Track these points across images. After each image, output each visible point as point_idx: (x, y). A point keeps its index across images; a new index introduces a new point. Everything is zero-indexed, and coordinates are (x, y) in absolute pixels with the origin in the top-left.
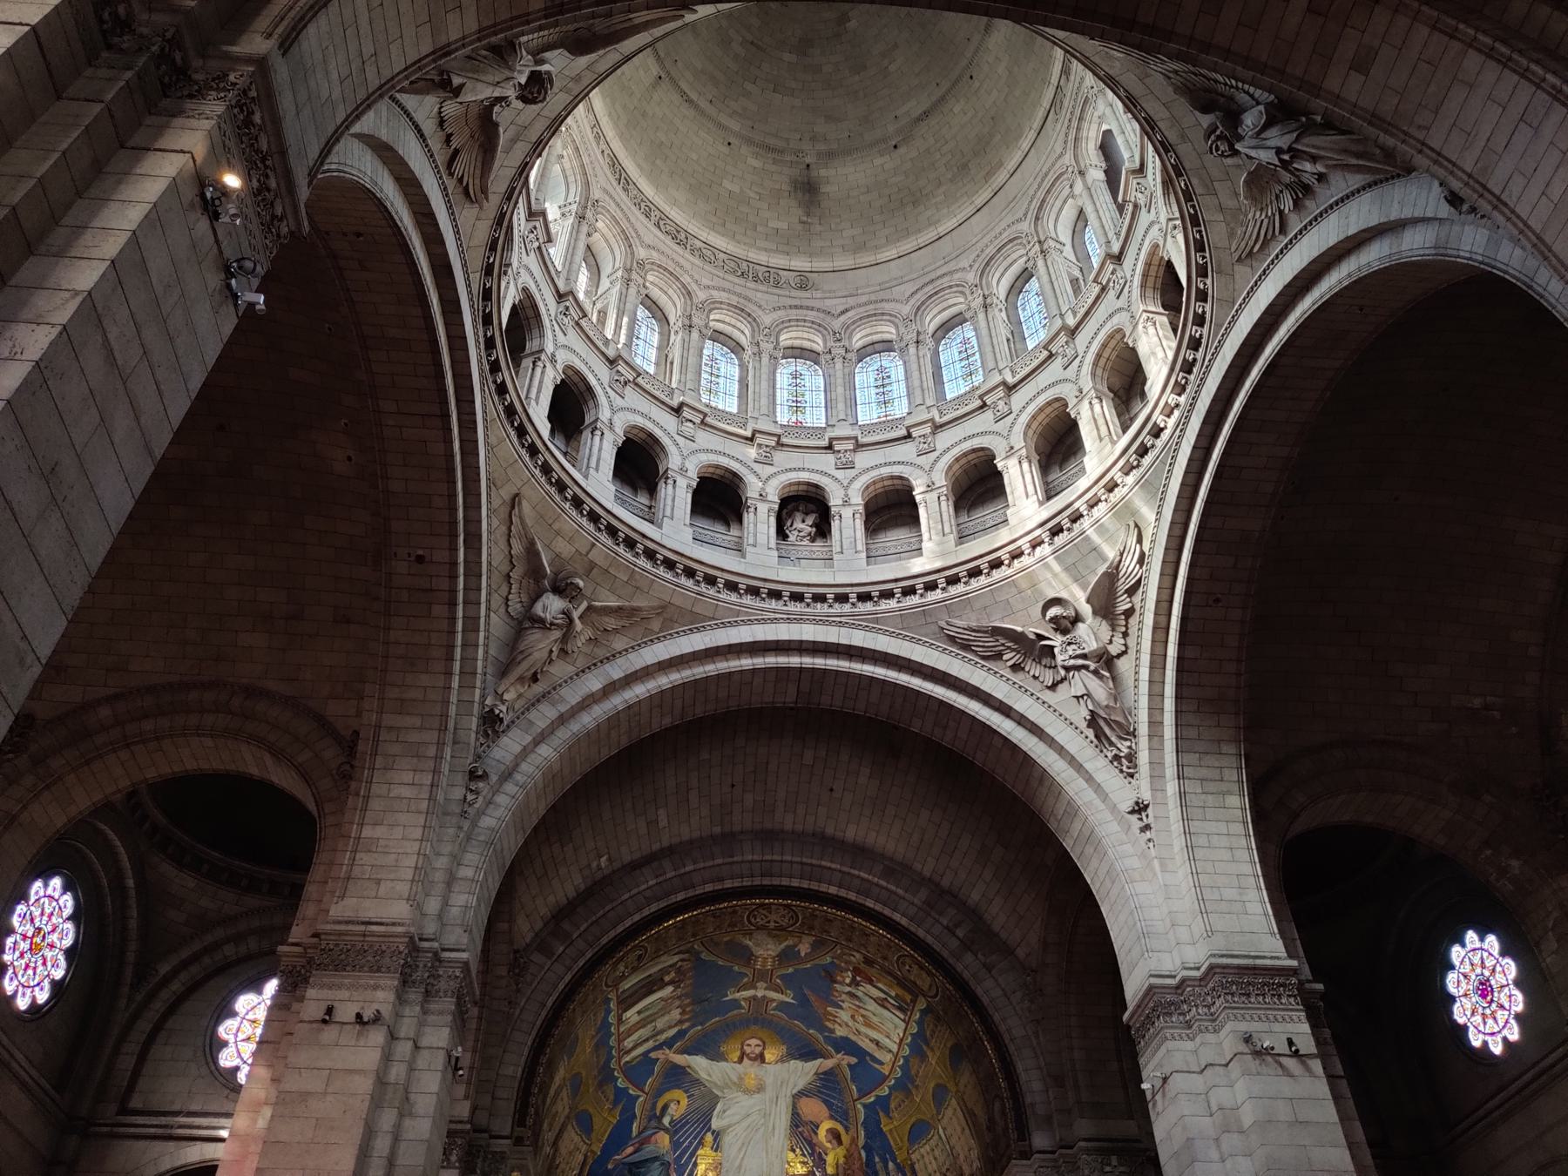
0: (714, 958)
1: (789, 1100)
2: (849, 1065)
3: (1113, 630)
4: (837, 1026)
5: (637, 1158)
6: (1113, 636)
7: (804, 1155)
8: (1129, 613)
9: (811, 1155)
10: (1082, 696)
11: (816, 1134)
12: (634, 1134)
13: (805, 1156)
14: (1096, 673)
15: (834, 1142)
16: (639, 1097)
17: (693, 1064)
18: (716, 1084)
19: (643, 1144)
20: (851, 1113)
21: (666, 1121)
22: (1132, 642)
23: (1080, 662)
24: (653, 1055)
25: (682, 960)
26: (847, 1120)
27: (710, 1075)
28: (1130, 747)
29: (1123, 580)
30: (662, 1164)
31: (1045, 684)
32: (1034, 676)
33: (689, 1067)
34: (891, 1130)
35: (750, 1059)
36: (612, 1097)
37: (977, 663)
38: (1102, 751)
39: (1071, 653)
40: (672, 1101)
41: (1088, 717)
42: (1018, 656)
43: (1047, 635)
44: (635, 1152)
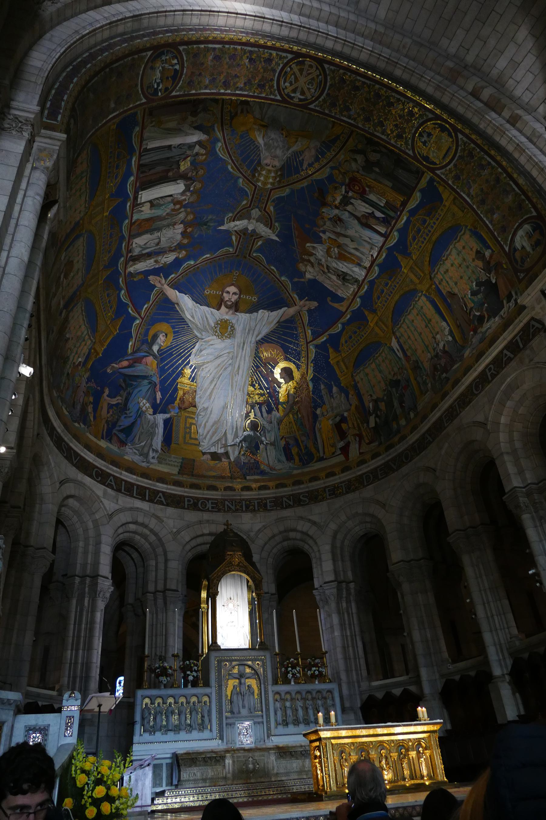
0: (226, 157)
1: (253, 345)
2: (310, 311)
4: (309, 268)
5: (129, 371)
7: (261, 388)
9: (266, 389)
11: (273, 373)
12: (130, 351)
13: (263, 390)
15: (287, 377)
16: (135, 319)
17: (181, 303)
18: (196, 326)
19: (135, 362)
20: (303, 354)
21: (155, 348)
24: (152, 279)
25: (199, 143)
26: (299, 360)
27: (193, 317)
30: (150, 383)
33: (178, 304)
34: (338, 362)
35: (227, 307)
36: (115, 306)
40: (162, 332)
44: (129, 366)
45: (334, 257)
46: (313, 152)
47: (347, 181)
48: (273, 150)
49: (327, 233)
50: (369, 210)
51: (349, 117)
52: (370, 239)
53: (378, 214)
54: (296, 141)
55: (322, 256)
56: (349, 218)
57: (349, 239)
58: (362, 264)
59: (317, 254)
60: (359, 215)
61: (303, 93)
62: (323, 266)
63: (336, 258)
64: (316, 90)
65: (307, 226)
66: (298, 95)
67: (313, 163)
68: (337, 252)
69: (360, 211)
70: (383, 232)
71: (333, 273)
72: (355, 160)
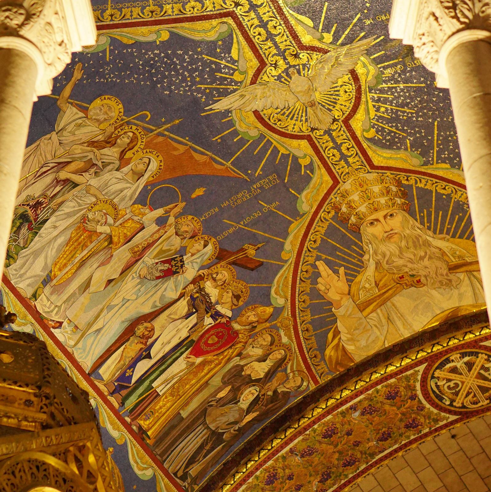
45: (90, 216)
46: (333, 295)
47: (236, 326)
48: (403, 244)
49: (154, 227)
50: (157, 352)
51: (354, 408)
52: (99, 331)
53: (143, 367)
54: (377, 285)
55: (106, 185)
56: (162, 297)
57: (116, 276)
58: (47, 290)
59: (118, 174)
60: (158, 323)
61: (454, 370)
62: (80, 172)
63: (84, 219)
64: (438, 387)
65: (199, 192)
66: (460, 364)
67: (315, 282)
68: (100, 229)
69: (163, 328)
70: (101, 371)
71: (50, 193)
72: (262, 359)
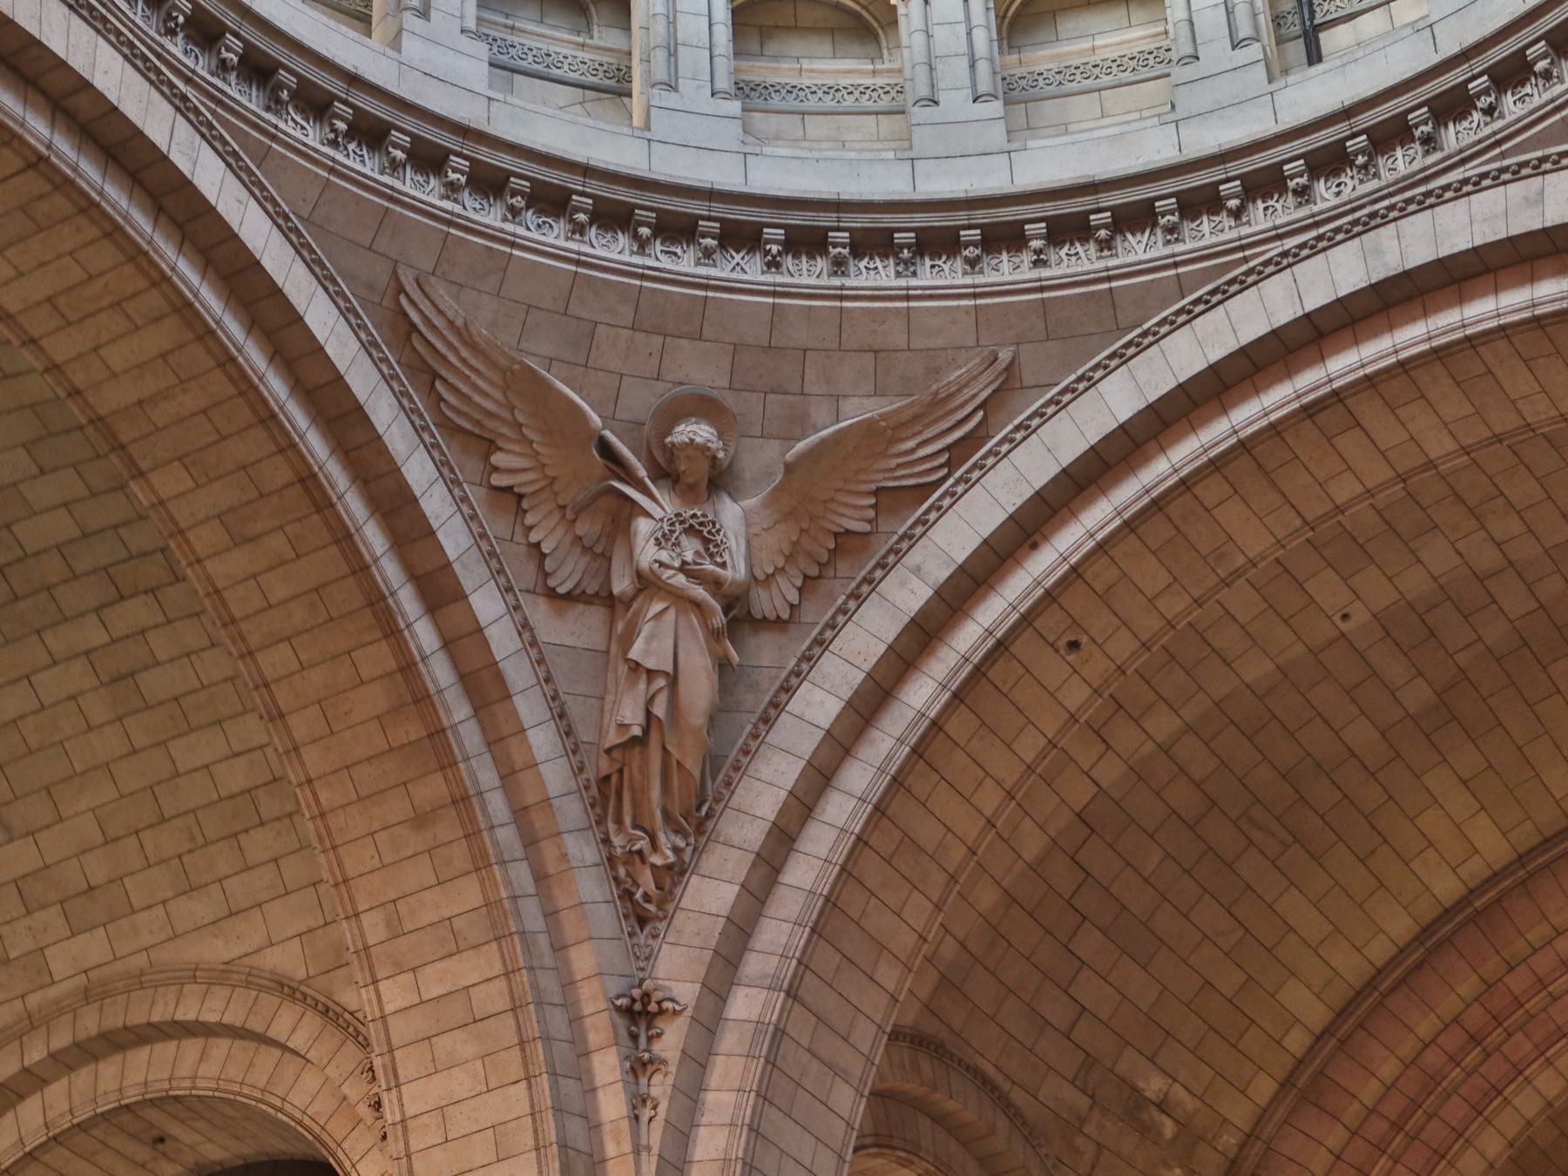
3: (790, 558)
6: (780, 570)
8: (846, 543)
10: (651, 674)
14: (715, 635)
22: (816, 615)
23: (700, 592)
28: (677, 850)
29: (894, 462)
31: (551, 583)
32: (537, 545)
37: (425, 428)
38: (601, 821)
39: (689, 557)
41: (636, 731)
42: (530, 476)
43: (642, 472)
